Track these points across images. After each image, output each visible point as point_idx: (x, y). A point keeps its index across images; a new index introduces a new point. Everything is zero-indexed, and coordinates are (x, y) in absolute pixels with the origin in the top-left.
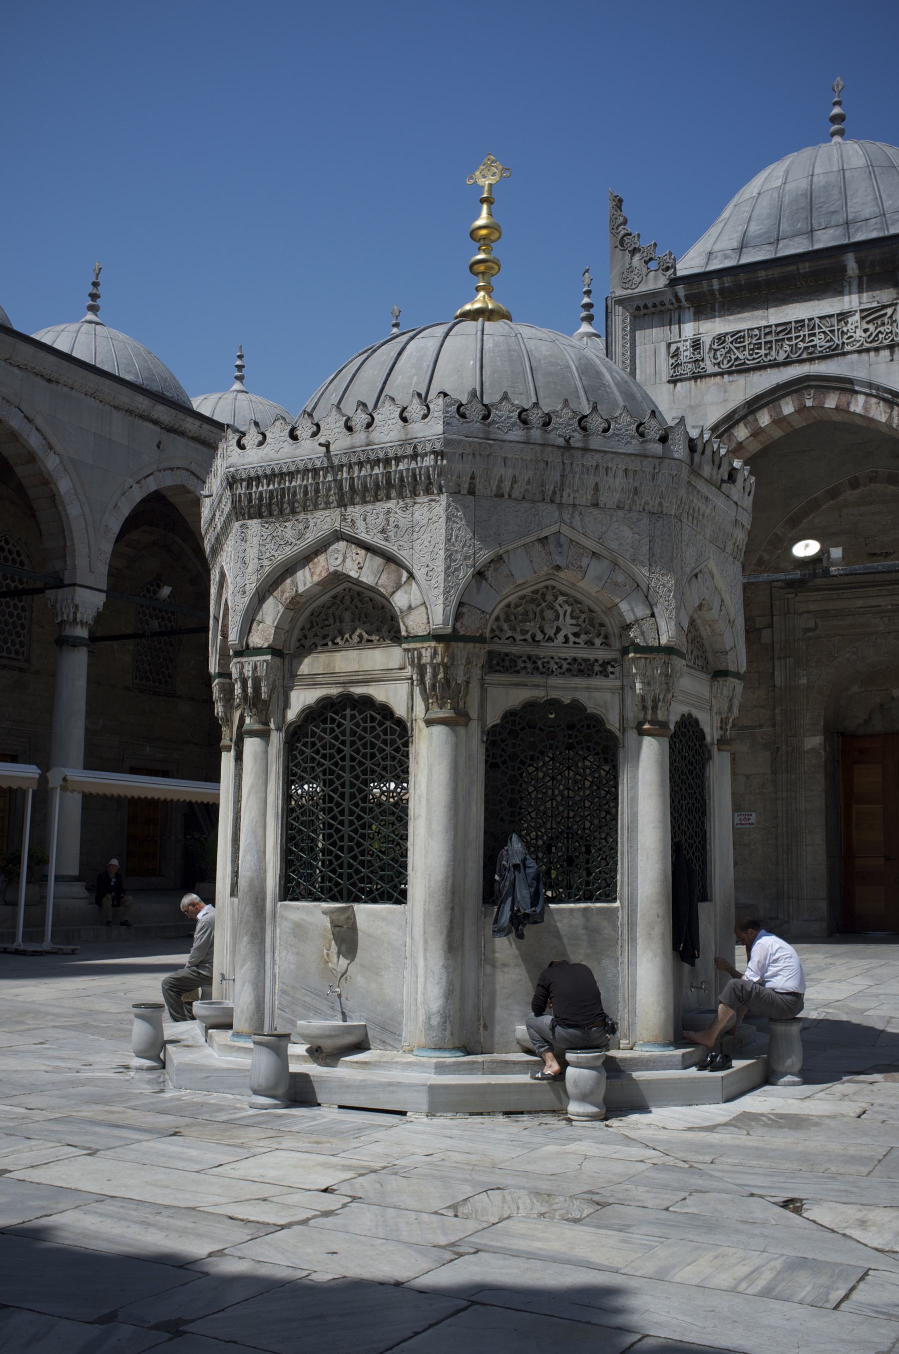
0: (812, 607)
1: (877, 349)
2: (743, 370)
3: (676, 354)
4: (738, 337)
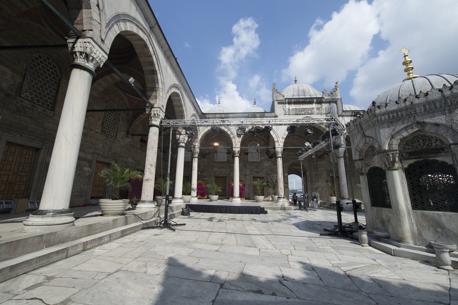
0: (286, 154)
1: (319, 114)
2: (297, 114)
3: (285, 110)
4: (296, 109)
